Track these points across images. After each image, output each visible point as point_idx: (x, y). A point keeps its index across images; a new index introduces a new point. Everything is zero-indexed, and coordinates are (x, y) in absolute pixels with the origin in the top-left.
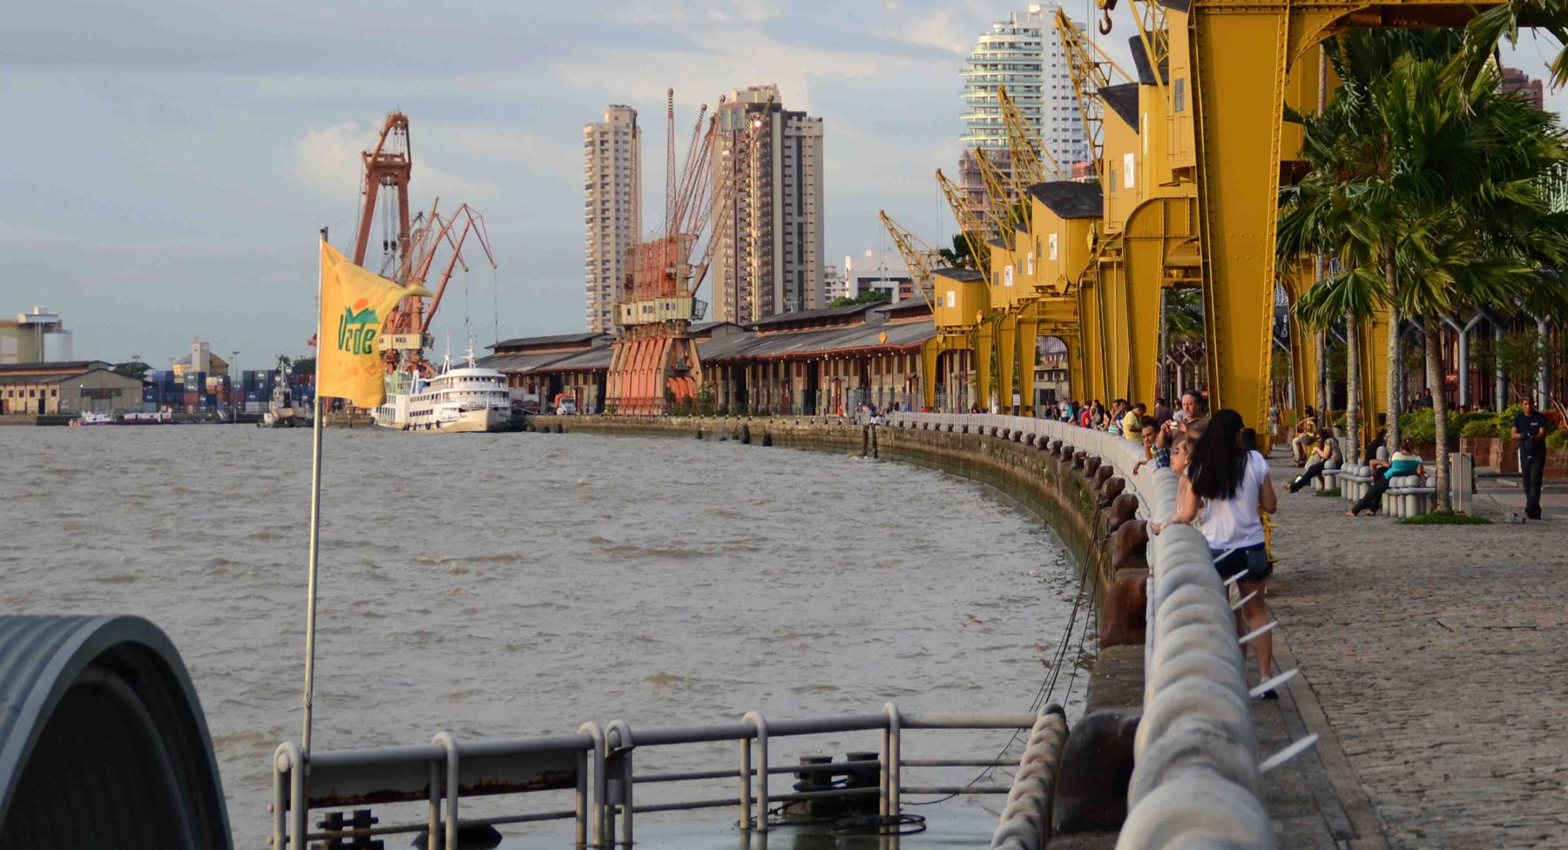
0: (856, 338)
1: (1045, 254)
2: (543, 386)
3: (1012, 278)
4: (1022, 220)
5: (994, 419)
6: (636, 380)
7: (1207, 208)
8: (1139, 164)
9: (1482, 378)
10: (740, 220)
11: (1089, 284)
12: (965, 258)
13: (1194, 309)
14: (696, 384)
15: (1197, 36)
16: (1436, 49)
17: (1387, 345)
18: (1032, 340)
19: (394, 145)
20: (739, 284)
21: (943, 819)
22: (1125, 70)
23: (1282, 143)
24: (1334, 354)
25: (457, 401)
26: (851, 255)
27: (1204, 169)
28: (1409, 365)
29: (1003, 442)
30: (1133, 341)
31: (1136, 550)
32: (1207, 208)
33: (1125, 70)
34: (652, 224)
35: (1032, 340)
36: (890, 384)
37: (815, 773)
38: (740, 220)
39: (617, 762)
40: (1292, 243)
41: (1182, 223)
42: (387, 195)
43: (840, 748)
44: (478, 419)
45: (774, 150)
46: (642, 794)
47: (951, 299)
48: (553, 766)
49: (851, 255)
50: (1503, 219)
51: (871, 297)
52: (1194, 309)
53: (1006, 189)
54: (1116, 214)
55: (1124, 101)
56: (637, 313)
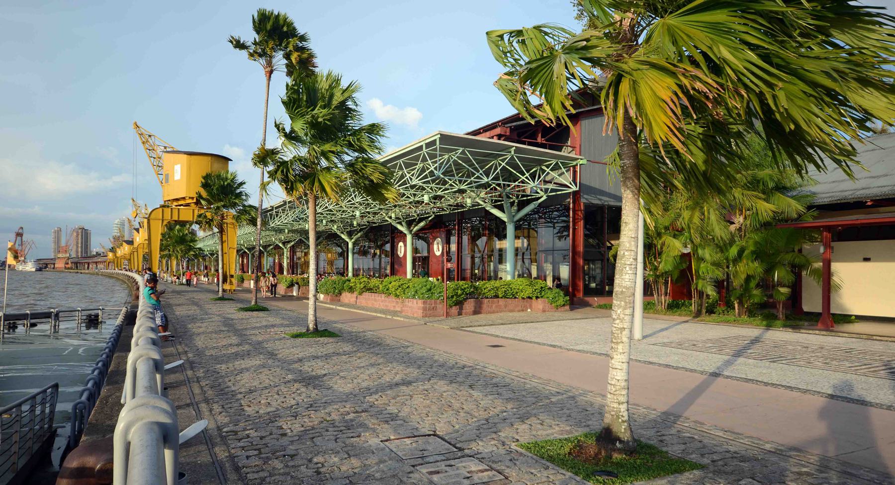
0: (95, 260)
1: (125, 249)
2: (43, 266)
3: (120, 252)
4: (122, 245)
5: (117, 271)
6: (60, 265)
7: (150, 244)
8: (140, 238)
9: (188, 268)
10: (77, 243)
11: (132, 253)
12: (113, 250)
13: (147, 258)
14: (69, 266)
15: (149, 223)
16: (181, 226)
17: (175, 263)
18: (123, 261)
19: (20, 231)
20: (77, 252)
21: (108, 322)
22: (138, 226)
23: (160, 237)
24: (167, 265)
25: (30, 267)
26: (95, 249)
27: (149, 239)
28: (178, 265)
29: (118, 274)
30: (138, 262)
31: (138, 289)
32: (150, 244)
33: (138, 226)
34: (63, 243)
35: (123, 261)
36: (101, 266)
37: (90, 316)
38: (77, 243)
39: (57, 315)
40: (161, 250)
41: (146, 246)
42: (19, 238)
43: (93, 313)
44: (34, 270)
45: (85, 235)
46: (60, 319)
47: (111, 255)
48: (47, 315)
49: (95, 249)
50: (191, 248)
51: (98, 254)
52: (147, 258)
53: (119, 241)
54: (136, 245)
55: (137, 230)
56: (60, 255)
